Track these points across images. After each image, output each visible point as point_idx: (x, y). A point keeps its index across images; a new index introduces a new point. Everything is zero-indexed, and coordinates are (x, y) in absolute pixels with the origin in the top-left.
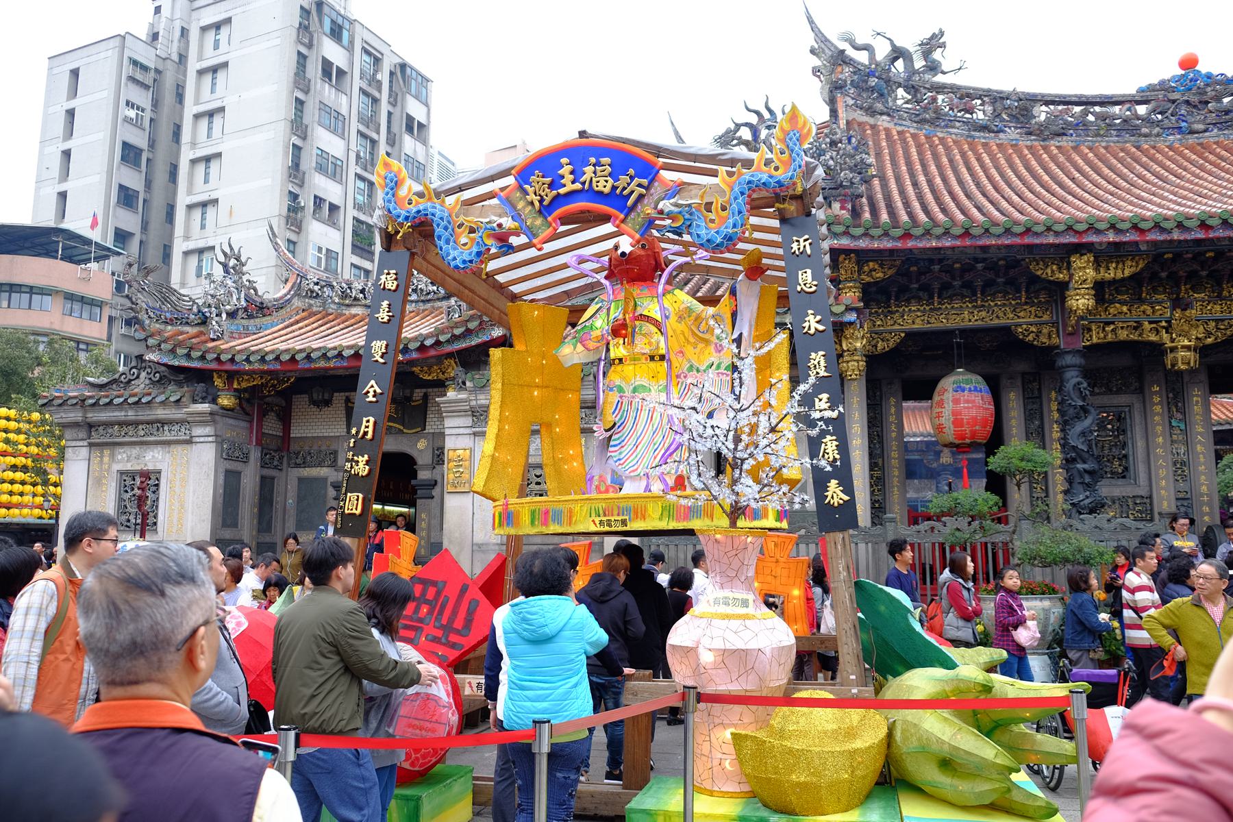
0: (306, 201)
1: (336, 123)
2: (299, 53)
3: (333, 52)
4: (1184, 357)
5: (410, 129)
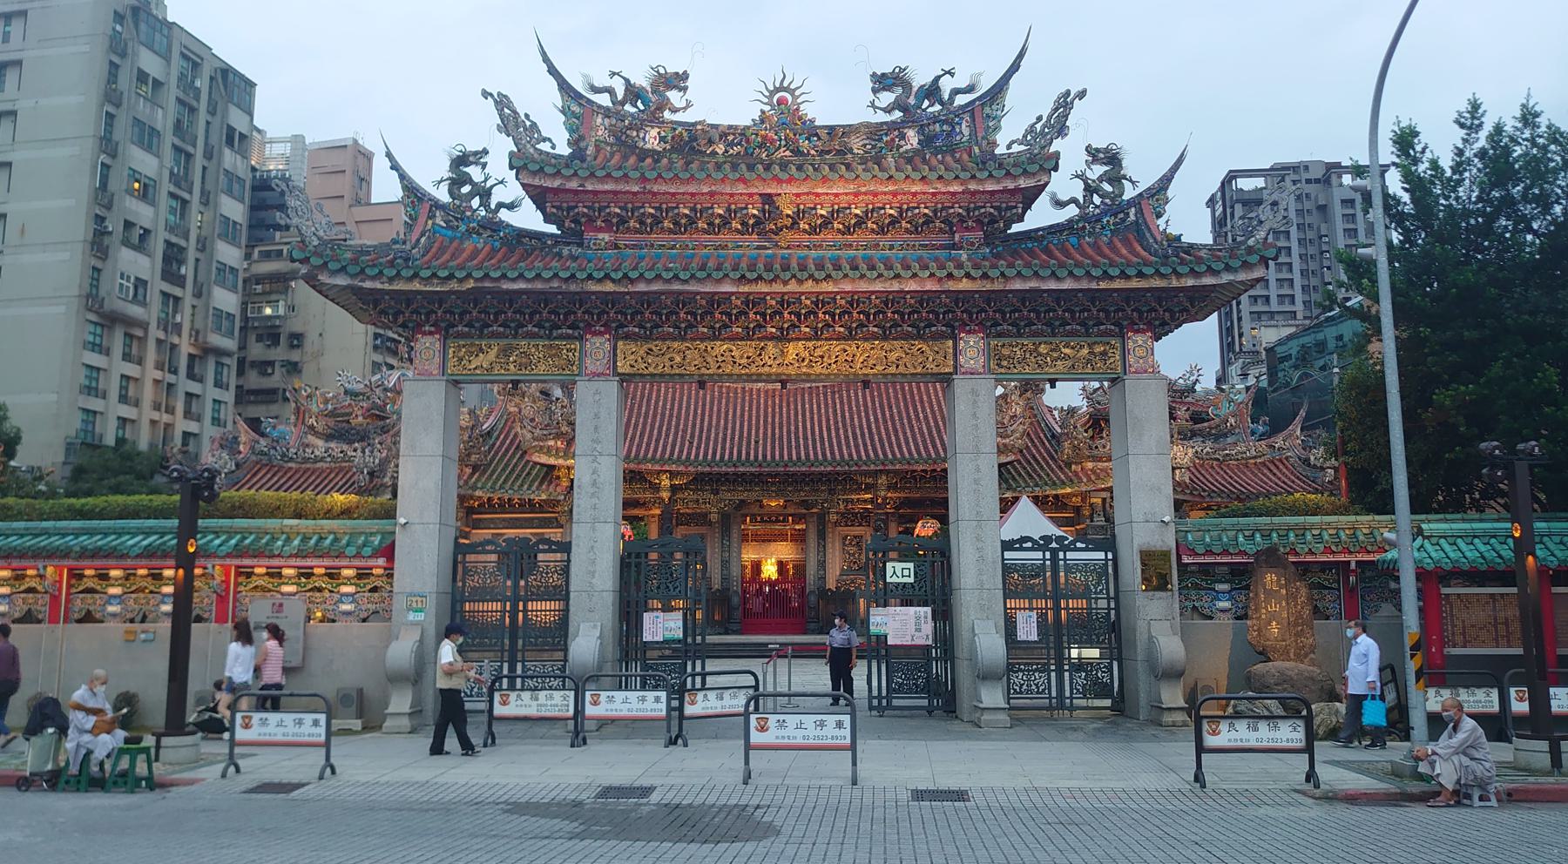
0: (114, 225)
1: (147, 137)
2: (111, 63)
3: (150, 63)
4: (714, 517)
5: (230, 142)
